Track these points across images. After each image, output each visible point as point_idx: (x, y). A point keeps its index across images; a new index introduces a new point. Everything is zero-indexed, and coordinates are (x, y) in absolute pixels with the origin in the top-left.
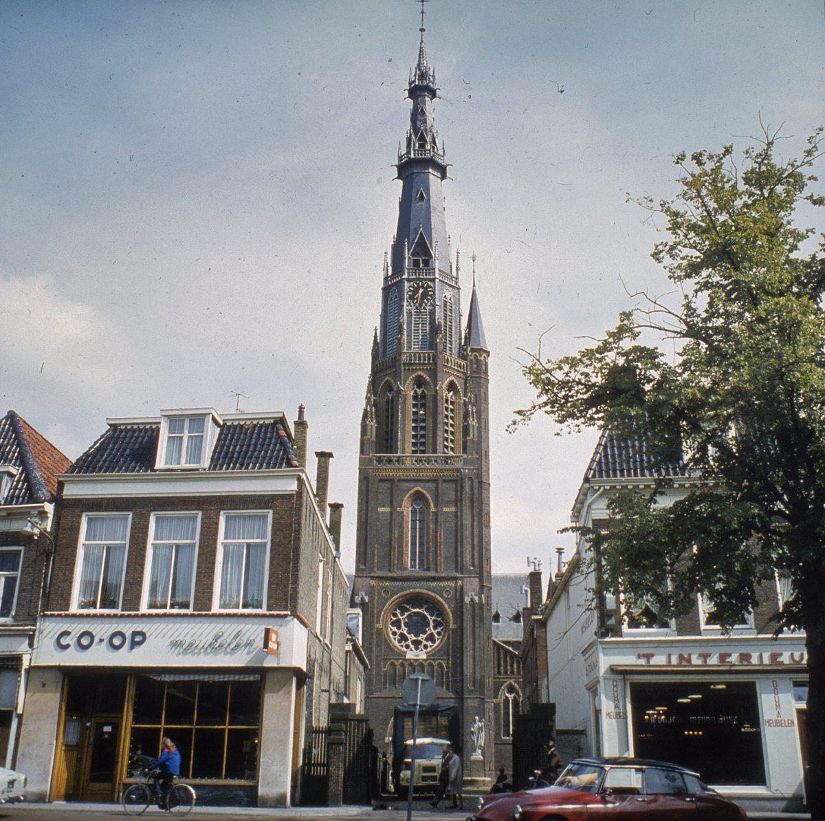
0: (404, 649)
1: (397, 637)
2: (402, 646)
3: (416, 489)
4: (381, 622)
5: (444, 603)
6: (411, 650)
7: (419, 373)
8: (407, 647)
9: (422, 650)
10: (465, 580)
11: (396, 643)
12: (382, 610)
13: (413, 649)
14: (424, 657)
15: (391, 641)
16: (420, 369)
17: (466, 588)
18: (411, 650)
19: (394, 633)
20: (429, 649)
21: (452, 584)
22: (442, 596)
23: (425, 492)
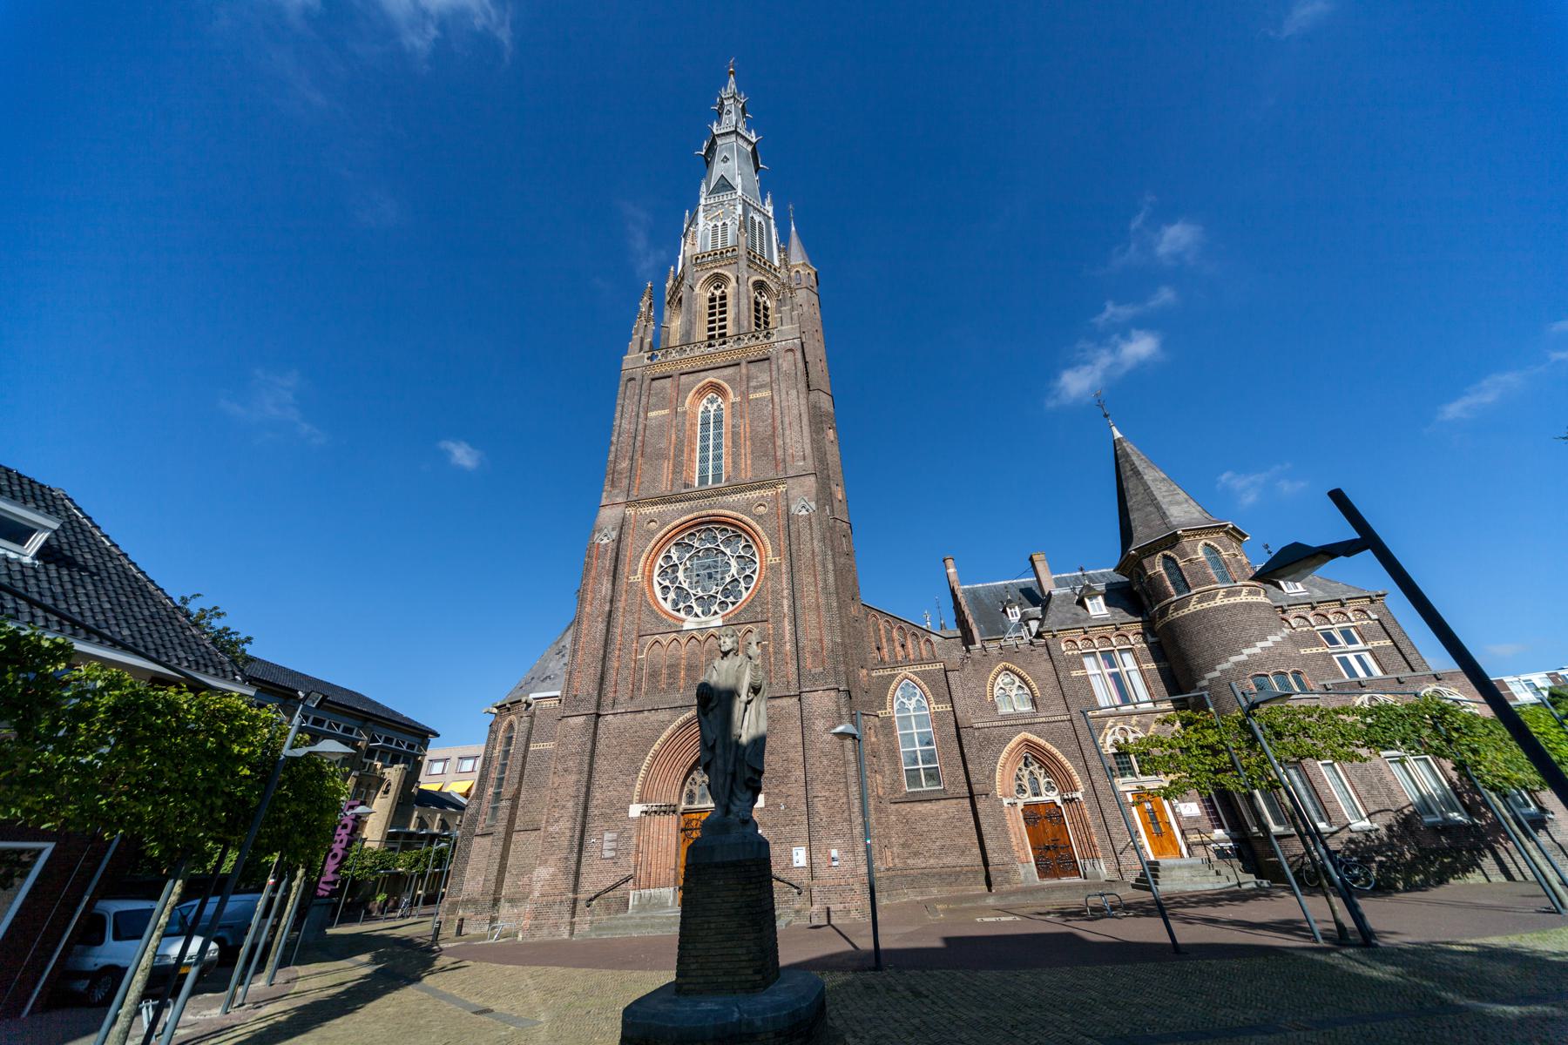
0: (682, 614)
1: (672, 595)
2: (679, 610)
3: (707, 380)
4: (640, 571)
5: (753, 524)
6: (697, 615)
7: (716, 271)
8: (689, 610)
9: (716, 613)
10: (790, 481)
11: (668, 606)
12: (643, 551)
13: (700, 613)
14: (720, 623)
15: (657, 603)
16: (716, 267)
17: (792, 493)
18: (697, 615)
19: (665, 589)
20: (731, 608)
21: (769, 493)
22: (750, 514)
23: (720, 382)
